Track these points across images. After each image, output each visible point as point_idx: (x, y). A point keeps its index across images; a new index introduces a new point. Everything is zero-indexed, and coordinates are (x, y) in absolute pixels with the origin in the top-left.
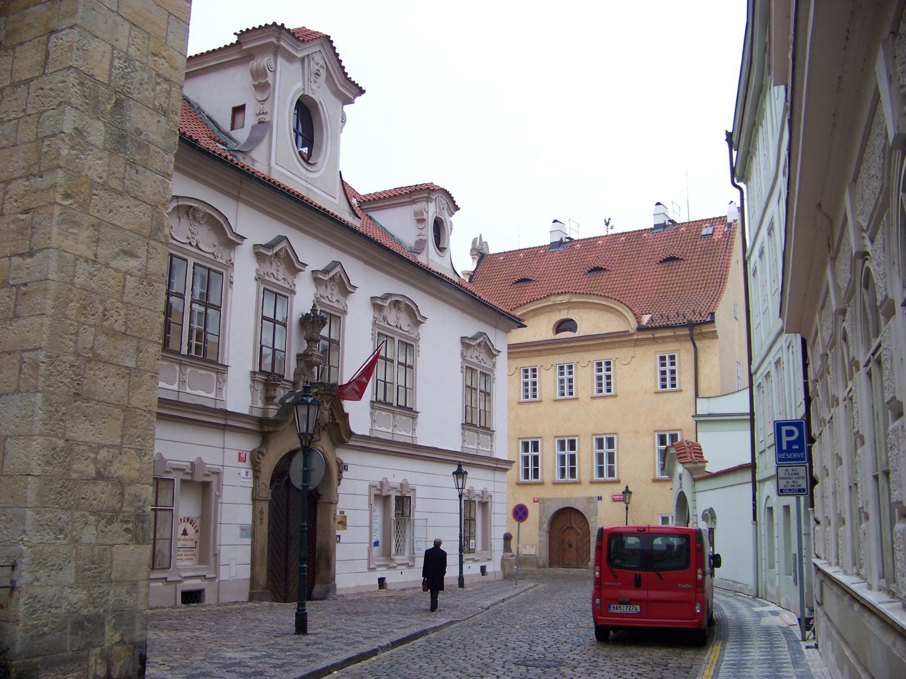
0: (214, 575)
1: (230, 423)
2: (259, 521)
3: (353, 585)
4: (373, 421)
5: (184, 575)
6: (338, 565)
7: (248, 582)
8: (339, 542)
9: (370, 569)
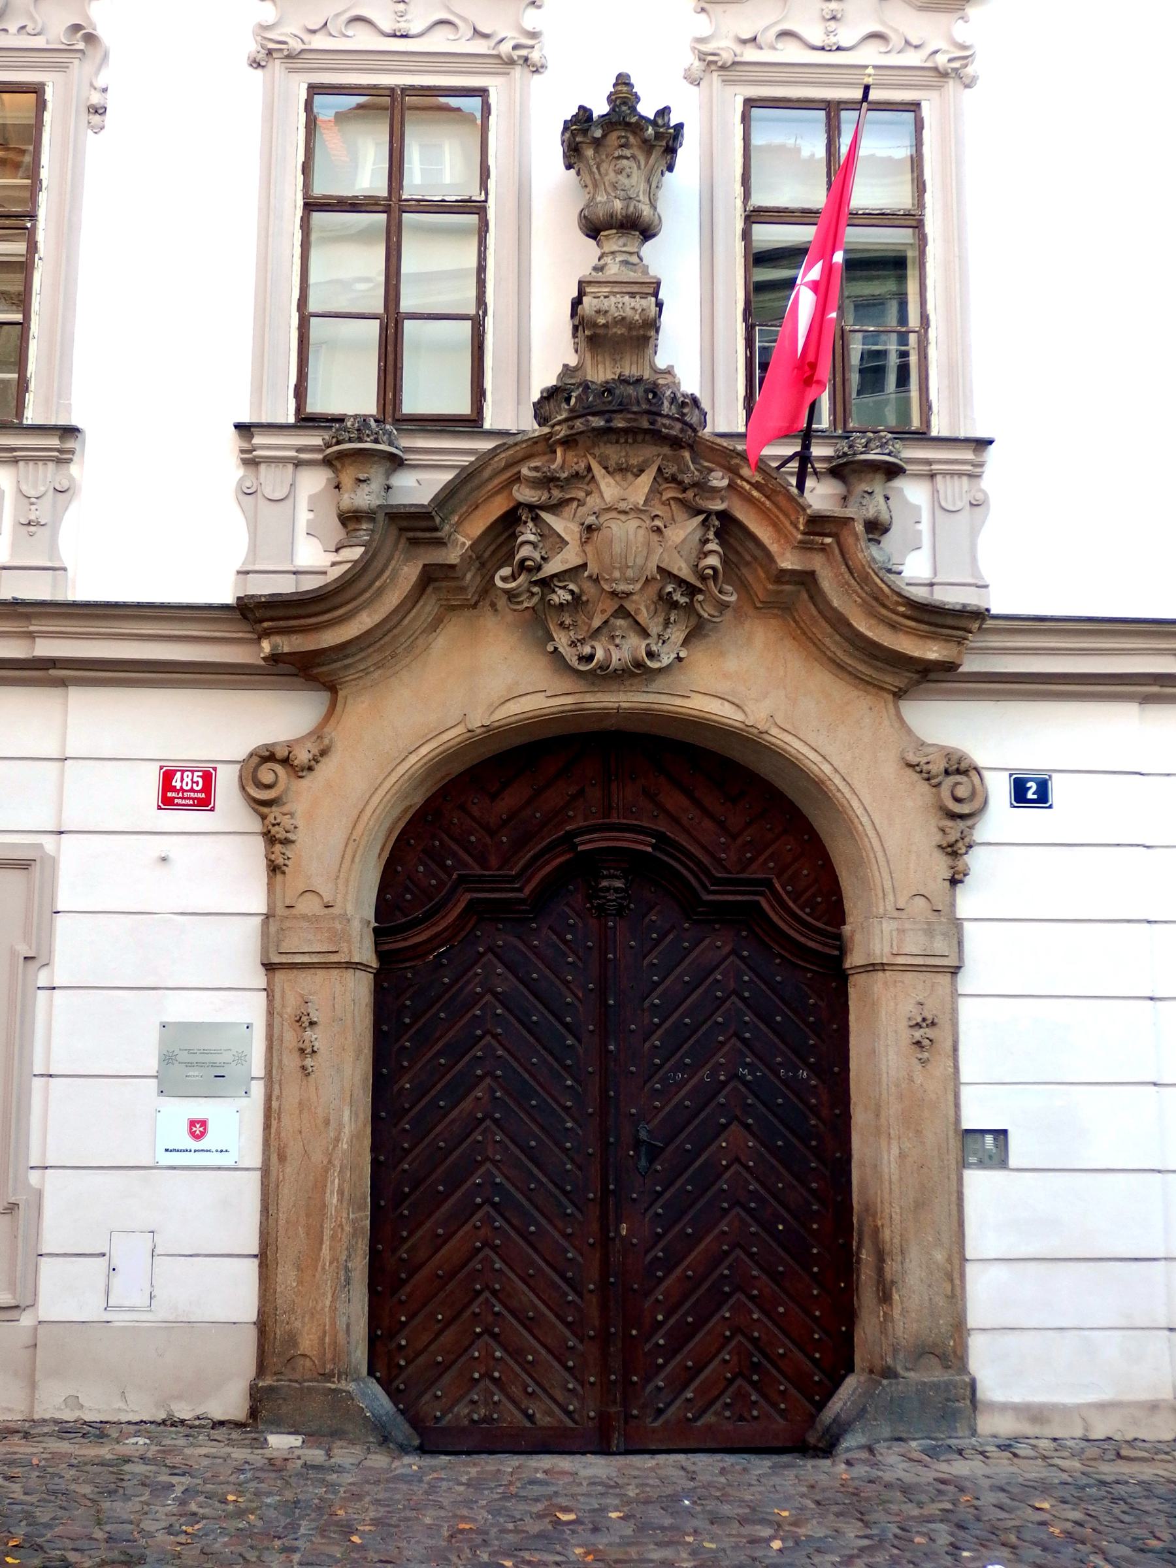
1: (46, 648)
2: (291, 1062)
7: (252, 1335)
8: (999, 1159)
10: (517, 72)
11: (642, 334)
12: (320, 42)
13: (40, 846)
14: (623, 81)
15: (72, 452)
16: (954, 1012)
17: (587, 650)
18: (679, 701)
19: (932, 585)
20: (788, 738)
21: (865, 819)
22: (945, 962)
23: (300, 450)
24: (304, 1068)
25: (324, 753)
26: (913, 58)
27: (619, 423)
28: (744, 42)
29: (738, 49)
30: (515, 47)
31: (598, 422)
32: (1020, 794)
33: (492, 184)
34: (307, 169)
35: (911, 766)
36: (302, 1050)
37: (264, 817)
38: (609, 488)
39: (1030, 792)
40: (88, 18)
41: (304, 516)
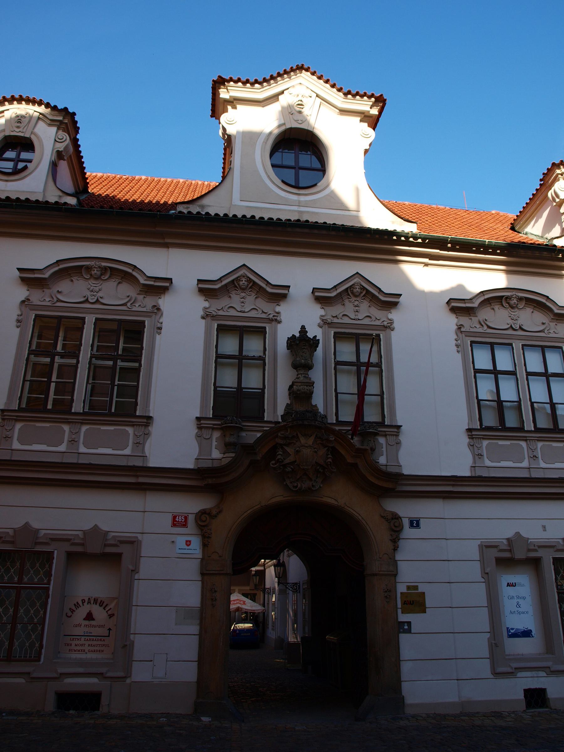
0: (121, 674)
1: (141, 480)
3: (453, 698)
4: (478, 456)
5: (61, 670)
6: (406, 668)
8: (409, 631)
9: (497, 674)
10: (274, 323)
11: (309, 395)
12: (221, 313)
13: (137, 537)
14: (303, 327)
15: (150, 423)
16: (396, 587)
17: (296, 484)
18: (320, 499)
19: (386, 465)
20: (350, 509)
21: (371, 532)
22: (393, 573)
23: (214, 425)
24: (212, 604)
25: (220, 512)
26: (378, 323)
27: (306, 423)
28: (334, 317)
29: (332, 319)
30: (273, 316)
31: (300, 422)
32: (411, 525)
33: (267, 352)
34: (217, 347)
35: (382, 517)
36: (212, 599)
37: (202, 530)
38: (303, 440)
39: (415, 523)
40: (158, 303)
41: (214, 443)
